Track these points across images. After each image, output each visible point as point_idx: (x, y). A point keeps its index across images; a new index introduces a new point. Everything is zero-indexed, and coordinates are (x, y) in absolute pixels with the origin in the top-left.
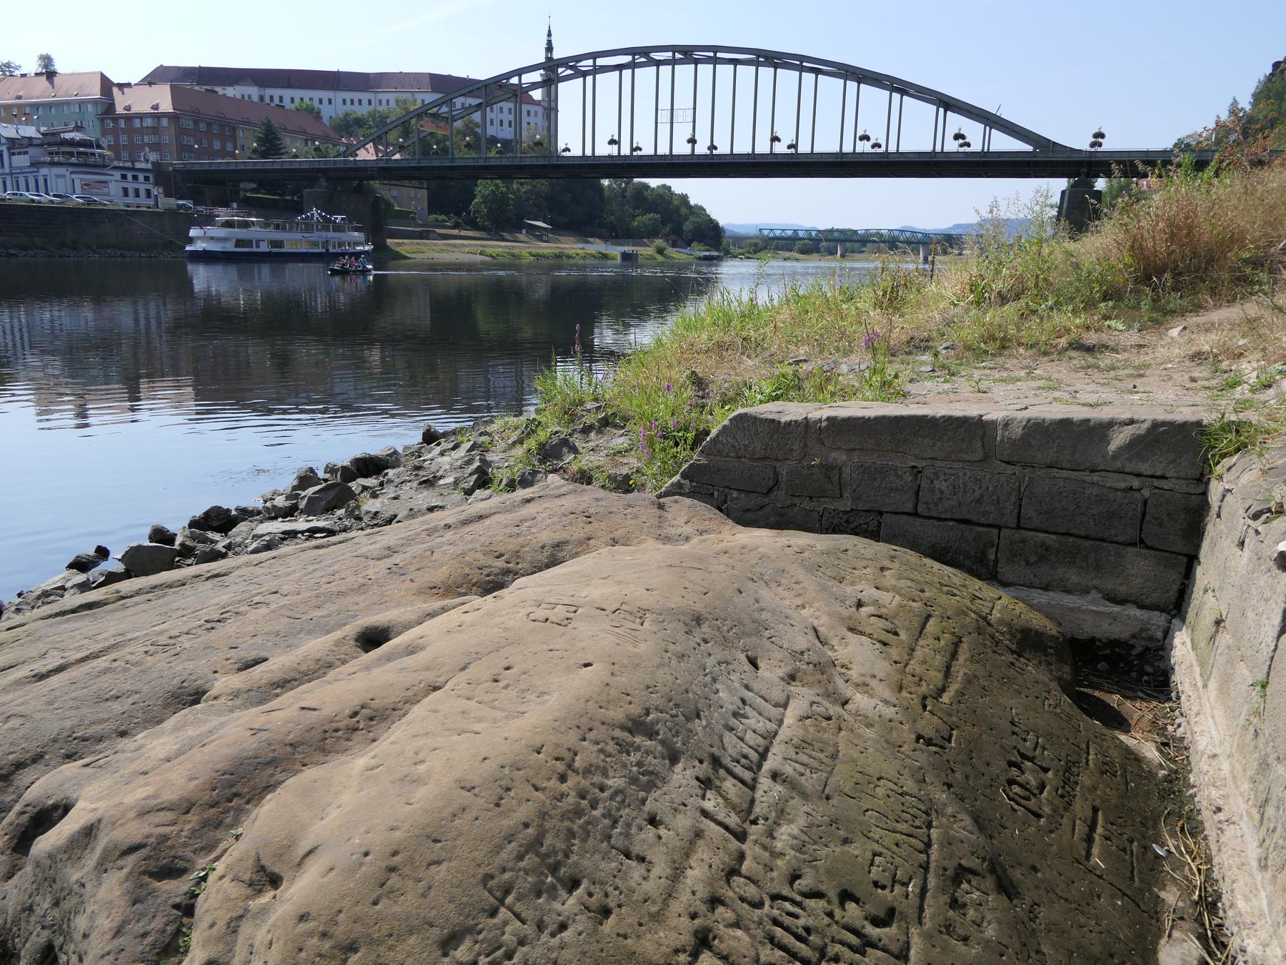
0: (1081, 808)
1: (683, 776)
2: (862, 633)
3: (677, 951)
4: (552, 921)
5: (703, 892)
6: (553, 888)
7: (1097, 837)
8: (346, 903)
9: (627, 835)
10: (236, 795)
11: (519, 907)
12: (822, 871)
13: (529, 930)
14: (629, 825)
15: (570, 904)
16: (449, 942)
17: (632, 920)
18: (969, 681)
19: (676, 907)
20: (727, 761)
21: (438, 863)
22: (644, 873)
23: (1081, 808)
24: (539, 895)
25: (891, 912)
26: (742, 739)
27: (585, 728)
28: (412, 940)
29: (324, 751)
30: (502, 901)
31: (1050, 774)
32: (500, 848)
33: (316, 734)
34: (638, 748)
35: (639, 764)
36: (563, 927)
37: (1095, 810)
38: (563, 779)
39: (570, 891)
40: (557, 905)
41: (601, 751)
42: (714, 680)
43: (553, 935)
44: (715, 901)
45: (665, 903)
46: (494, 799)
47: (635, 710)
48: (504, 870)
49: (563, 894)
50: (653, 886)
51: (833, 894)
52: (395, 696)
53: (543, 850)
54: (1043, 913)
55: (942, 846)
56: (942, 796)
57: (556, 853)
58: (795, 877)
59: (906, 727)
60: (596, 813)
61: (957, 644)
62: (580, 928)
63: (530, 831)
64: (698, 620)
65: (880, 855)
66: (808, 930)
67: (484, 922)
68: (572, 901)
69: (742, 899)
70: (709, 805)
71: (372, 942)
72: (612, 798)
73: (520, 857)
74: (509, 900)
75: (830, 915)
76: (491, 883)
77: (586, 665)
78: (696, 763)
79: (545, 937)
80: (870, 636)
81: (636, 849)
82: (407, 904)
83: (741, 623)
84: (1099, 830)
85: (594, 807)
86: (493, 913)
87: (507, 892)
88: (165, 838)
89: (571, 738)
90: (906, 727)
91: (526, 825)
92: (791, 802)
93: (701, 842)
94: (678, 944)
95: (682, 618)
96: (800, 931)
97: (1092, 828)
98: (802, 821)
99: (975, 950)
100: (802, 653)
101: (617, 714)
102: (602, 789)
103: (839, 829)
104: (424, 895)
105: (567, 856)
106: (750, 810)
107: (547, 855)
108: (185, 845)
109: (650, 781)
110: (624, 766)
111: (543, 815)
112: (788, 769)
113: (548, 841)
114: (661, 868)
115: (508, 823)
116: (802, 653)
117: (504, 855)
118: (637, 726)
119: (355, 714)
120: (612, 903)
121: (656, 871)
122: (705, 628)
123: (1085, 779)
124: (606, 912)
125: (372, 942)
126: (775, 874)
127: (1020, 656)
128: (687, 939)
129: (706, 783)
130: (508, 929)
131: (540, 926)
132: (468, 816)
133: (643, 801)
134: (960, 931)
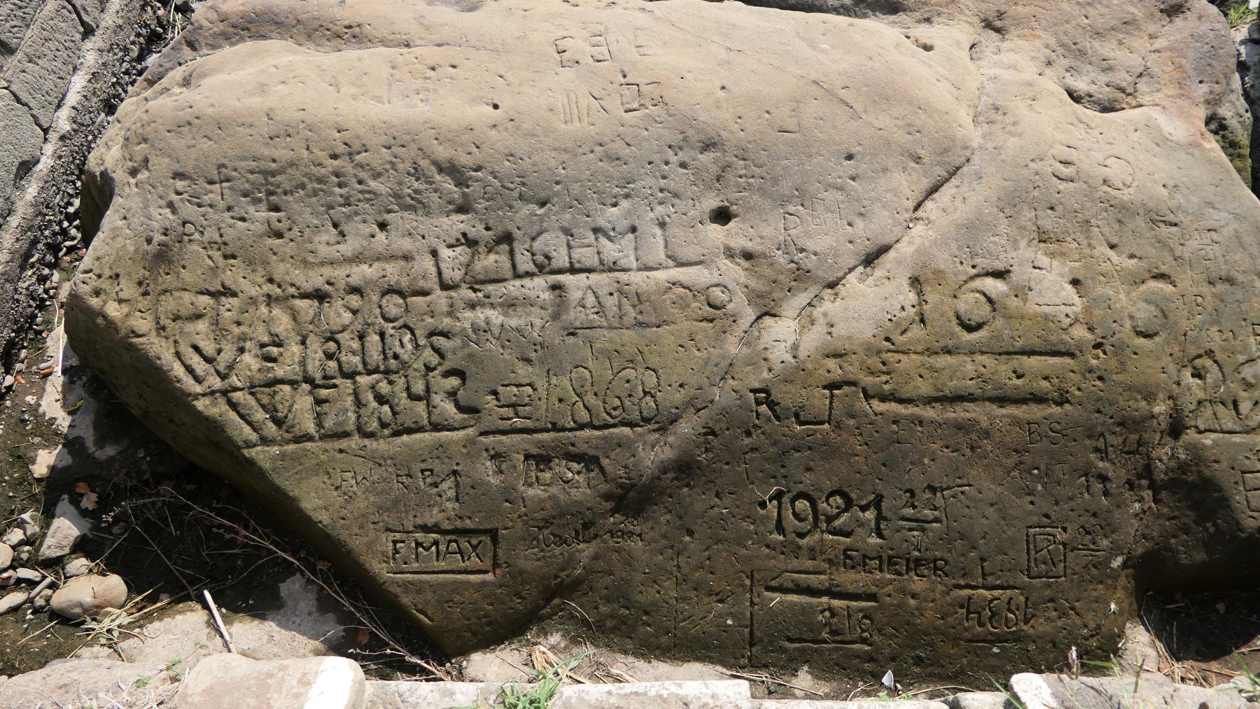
0: (850, 579)
1: (457, 224)
2: (920, 293)
3: (292, 285)
4: (238, 211)
5: (355, 280)
6: (260, 200)
7: (825, 599)
8: (160, 121)
9: (349, 217)
10: (248, 29)
11: (226, 192)
12: (466, 351)
13: (222, 205)
14: (357, 214)
15: (261, 214)
16: (177, 175)
17: (289, 252)
18: (960, 427)
19: (328, 272)
20: (517, 246)
21: (210, 139)
22: (333, 240)
23: (850, 579)
24: (245, 196)
25: (472, 410)
26: (569, 247)
27: (399, 142)
28: (166, 160)
29: (309, 36)
30: (221, 182)
31: (874, 540)
32: (246, 159)
33: (316, 24)
34: (431, 183)
35: (416, 191)
36: (243, 219)
37: (872, 597)
38: (334, 157)
39: (270, 210)
40: (251, 209)
41: (392, 163)
42: (627, 196)
43: (233, 218)
44: (355, 290)
45: (322, 264)
46: (273, 134)
47: (463, 159)
48: (236, 170)
49: (263, 206)
50: (324, 251)
51: (447, 365)
52: (383, 32)
53: (271, 180)
54: (636, 545)
55: (604, 438)
56: (687, 427)
57: (278, 186)
58: (445, 334)
59: (765, 375)
60: (337, 190)
61: (1038, 399)
62: (252, 227)
63: (273, 165)
64: (707, 146)
65: (535, 390)
66: (396, 357)
67: (201, 182)
68: (264, 214)
69: (380, 307)
70: (445, 253)
71: (152, 145)
72: (361, 192)
73: (252, 172)
74: (225, 184)
75: (429, 369)
76: (223, 170)
77: (496, 107)
78: (481, 227)
79: (227, 215)
80: (922, 301)
81: (343, 227)
82: (178, 143)
83: (775, 181)
84: (836, 603)
85: (340, 186)
86: (211, 182)
87: (228, 180)
88: (201, 27)
89: (373, 140)
90: (765, 375)
91: (274, 161)
92: (536, 310)
93: (403, 263)
94: (298, 284)
95: (690, 132)
96: (390, 354)
97: (830, 593)
98: (514, 322)
99: (494, 481)
100: (802, 250)
101: (443, 153)
102: (360, 182)
103: (533, 352)
104: (189, 147)
105: (285, 193)
106: (483, 282)
107: (272, 184)
108: (205, 37)
109: (416, 205)
110: (400, 183)
111: (292, 164)
112: (575, 295)
113: (279, 178)
114: (347, 249)
115: (266, 152)
116: (802, 250)
117: (243, 164)
118: (451, 170)
119: (350, 27)
120: (288, 235)
121: (341, 247)
122: (706, 158)
123: (918, 584)
124: (279, 235)
125: (152, 145)
126: (430, 320)
127: (1153, 486)
128: (308, 287)
129: (470, 242)
130: (211, 195)
131: (229, 209)
132: (249, 131)
133: (389, 211)
134: (504, 466)
